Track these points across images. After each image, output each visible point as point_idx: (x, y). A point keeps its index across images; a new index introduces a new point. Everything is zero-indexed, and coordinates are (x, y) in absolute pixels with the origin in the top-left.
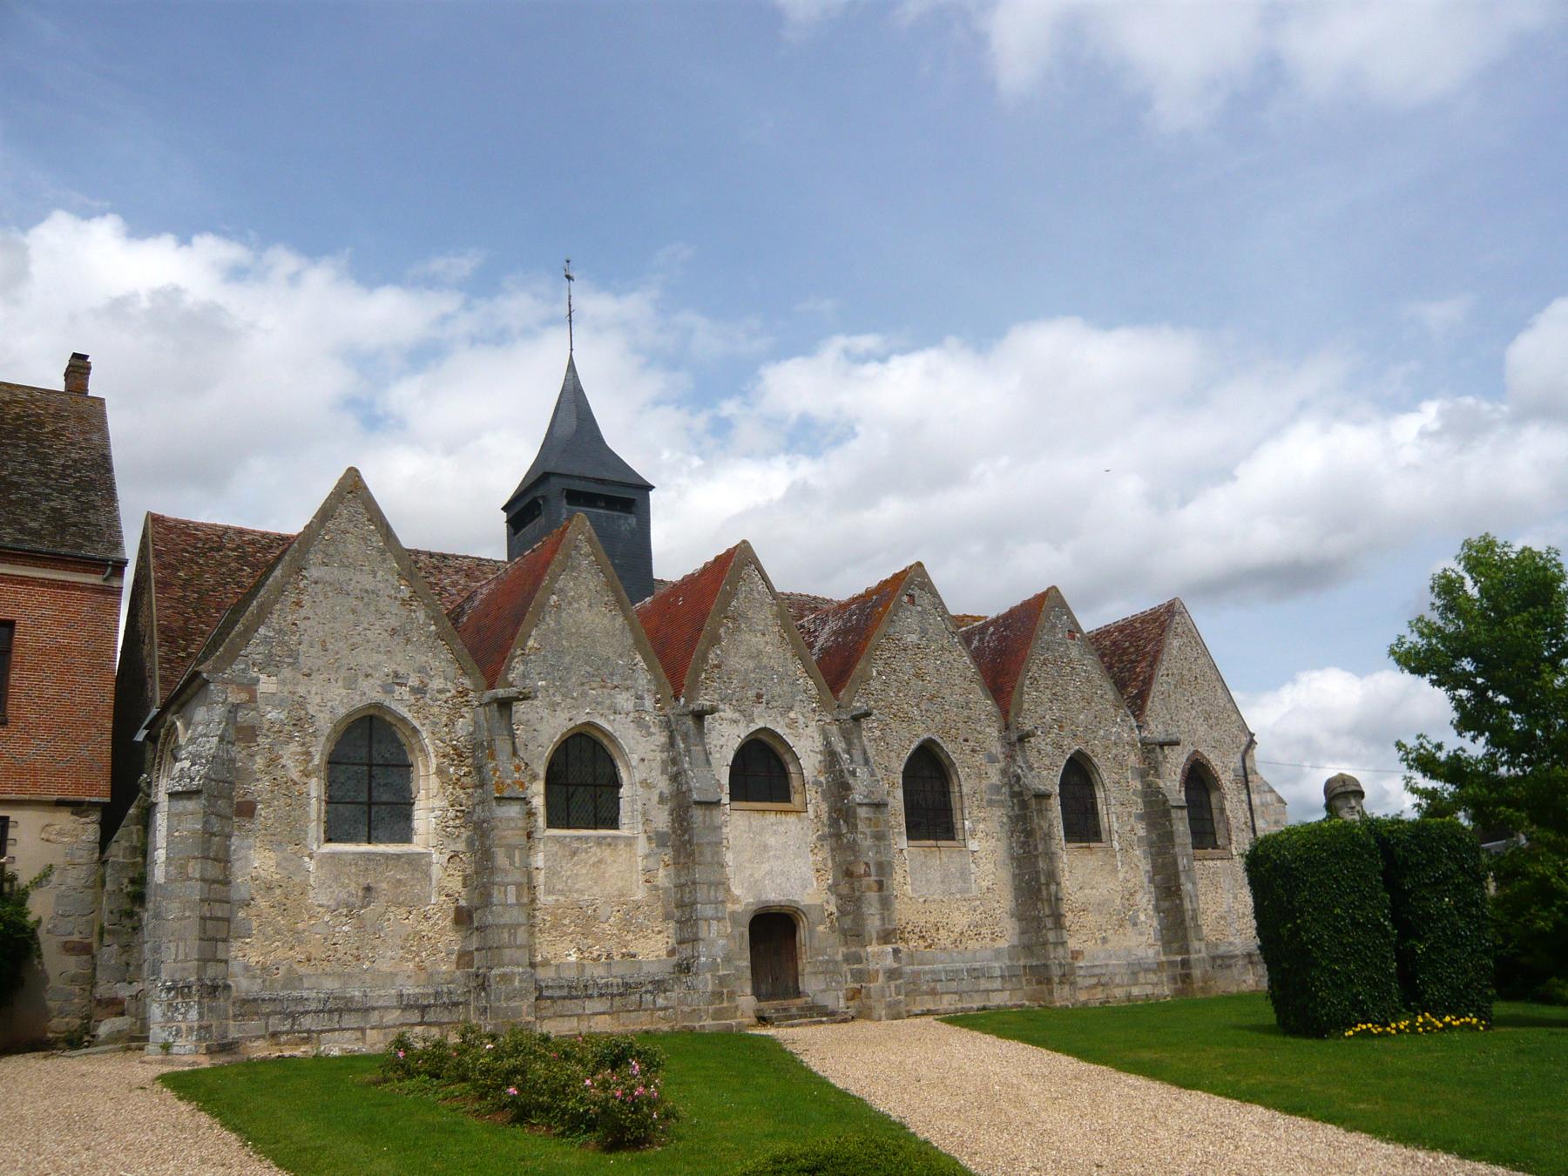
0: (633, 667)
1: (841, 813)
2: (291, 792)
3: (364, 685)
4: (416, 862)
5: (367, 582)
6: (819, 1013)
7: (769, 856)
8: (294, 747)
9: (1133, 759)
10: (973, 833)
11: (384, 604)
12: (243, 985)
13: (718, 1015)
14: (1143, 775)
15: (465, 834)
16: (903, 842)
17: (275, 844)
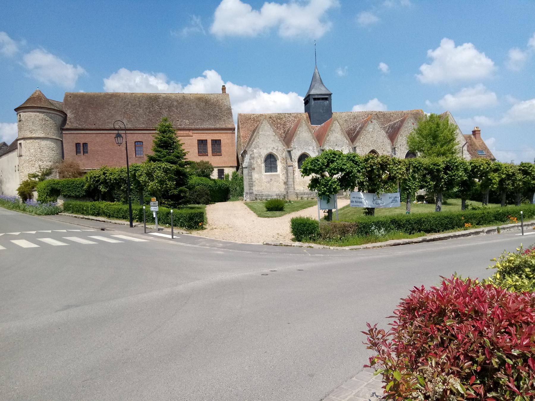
2: (259, 166)
5: (268, 133)
12: (255, 193)
17: (258, 174)
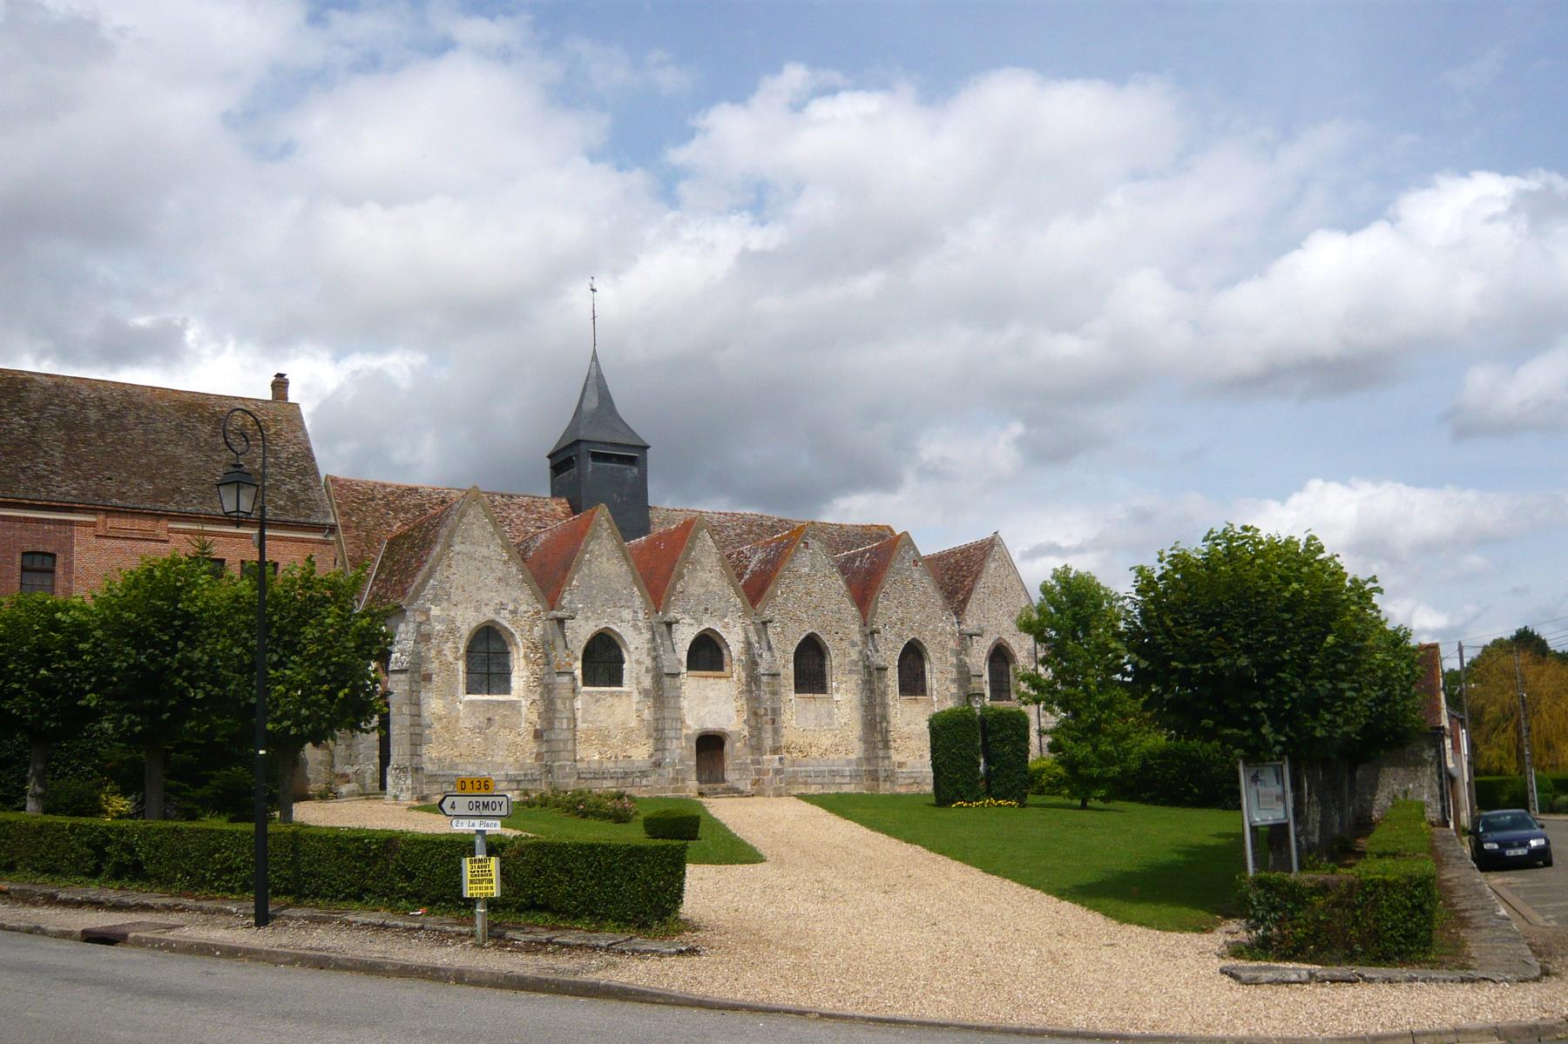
0: (632, 595)
1: (753, 679)
3: (485, 610)
4: (513, 705)
5: (485, 552)
6: (734, 792)
7: (711, 703)
8: (450, 644)
9: (952, 644)
10: (837, 690)
11: (494, 564)
12: (429, 767)
13: (675, 790)
14: (958, 654)
15: (539, 690)
16: (792, 695)
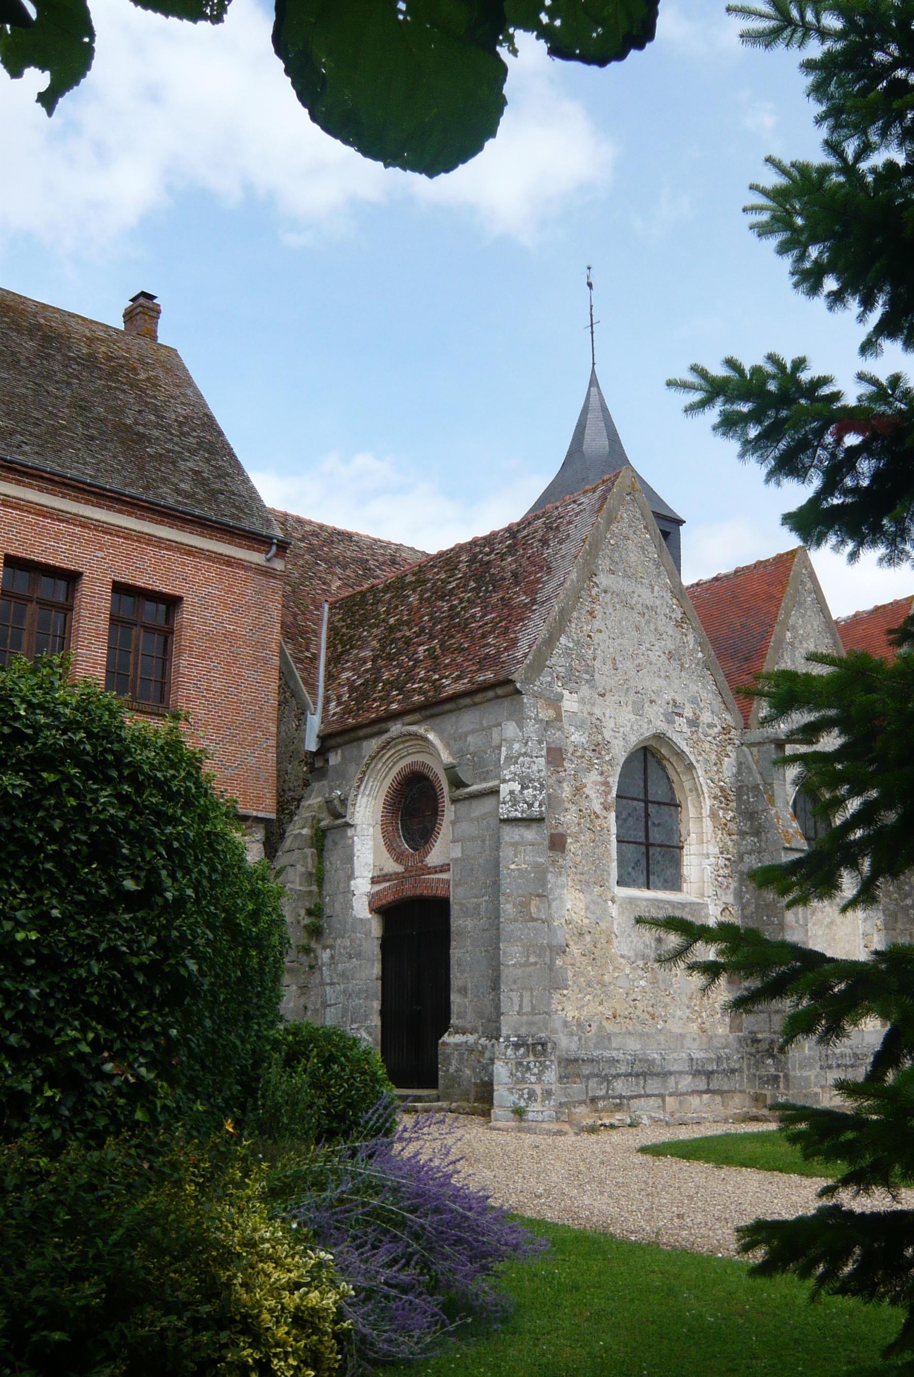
3: (651, 711)
11: (661, 621)
12: (566, 1043)
17: (584, 886)
